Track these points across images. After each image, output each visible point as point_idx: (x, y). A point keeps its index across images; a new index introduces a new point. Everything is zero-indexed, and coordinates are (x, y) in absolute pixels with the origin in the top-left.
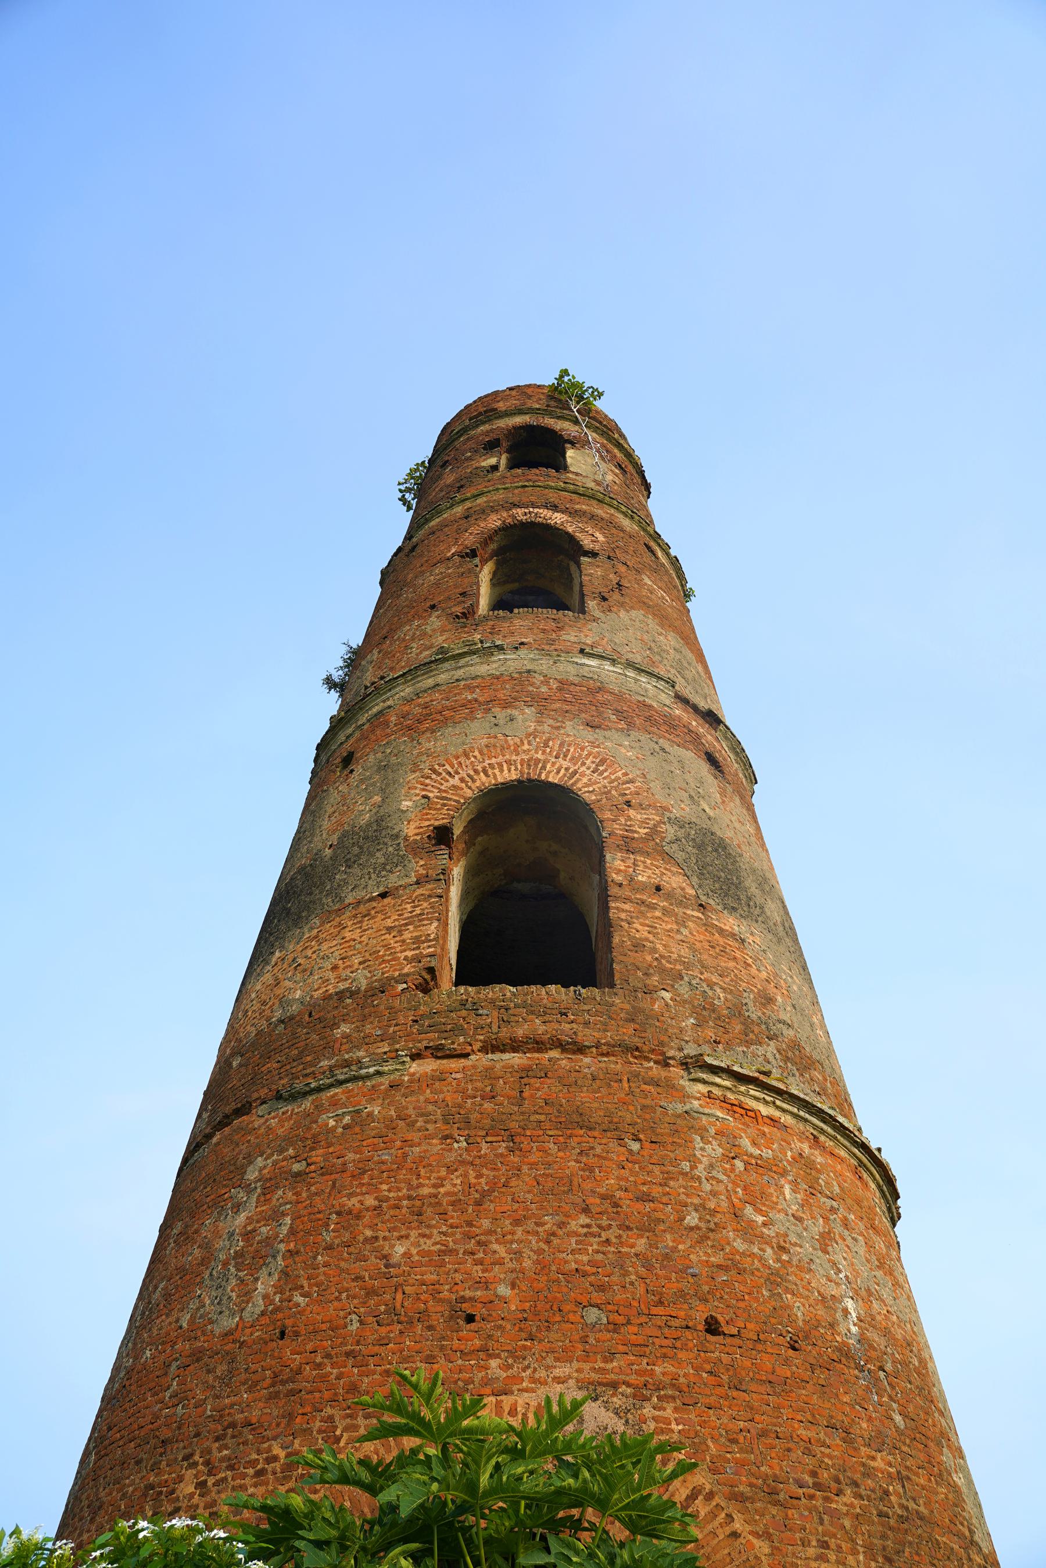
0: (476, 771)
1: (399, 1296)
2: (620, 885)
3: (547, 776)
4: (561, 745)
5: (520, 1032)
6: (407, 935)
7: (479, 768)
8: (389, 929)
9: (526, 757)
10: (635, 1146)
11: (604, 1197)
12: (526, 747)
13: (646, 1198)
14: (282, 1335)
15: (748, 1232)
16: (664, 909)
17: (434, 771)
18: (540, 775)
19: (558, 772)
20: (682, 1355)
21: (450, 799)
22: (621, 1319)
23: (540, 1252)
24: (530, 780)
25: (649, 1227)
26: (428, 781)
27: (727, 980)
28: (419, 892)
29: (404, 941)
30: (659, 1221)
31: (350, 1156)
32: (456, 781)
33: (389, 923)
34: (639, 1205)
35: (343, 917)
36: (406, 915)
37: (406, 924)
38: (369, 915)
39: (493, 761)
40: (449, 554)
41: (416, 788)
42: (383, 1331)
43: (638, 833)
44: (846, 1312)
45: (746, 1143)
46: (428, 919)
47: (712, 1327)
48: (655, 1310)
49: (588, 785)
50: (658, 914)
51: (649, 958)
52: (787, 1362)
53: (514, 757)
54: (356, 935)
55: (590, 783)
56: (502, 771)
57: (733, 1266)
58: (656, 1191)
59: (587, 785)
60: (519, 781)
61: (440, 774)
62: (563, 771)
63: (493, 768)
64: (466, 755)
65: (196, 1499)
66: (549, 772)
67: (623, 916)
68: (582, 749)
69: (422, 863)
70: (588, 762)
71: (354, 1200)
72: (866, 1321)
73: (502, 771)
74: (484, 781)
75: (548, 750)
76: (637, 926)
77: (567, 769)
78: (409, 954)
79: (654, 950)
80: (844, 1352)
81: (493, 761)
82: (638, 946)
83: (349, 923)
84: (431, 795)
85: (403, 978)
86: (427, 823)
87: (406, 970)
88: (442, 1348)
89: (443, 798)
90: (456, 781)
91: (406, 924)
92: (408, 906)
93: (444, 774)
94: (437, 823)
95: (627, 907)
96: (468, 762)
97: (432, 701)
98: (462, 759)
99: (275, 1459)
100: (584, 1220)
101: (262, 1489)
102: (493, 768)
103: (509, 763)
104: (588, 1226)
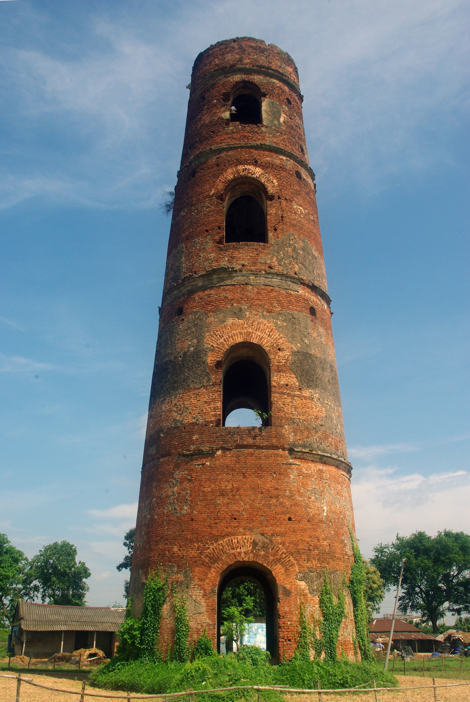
0: (229, 336)
1: (219, 514)
2: (275, 387)
3: (253, 341)
4: (258, 325)
5: (245, 443)
6: (211, 406)
7: (230, 335)
8: (206, 402)
9: (246, 331)
10: (275, 476)
11: (266, 490)
12: (246, 326)
13: (277, 489)
14: (192, 520)
15: (301, 495)
16: (288, 394)
17: (214, 333)
18: (250, 340)
19: (257, 338)
20: (282, 526)
21: (221, 349)
22: (269, 519)
23: (251, 504)
24: (247, 342)
25: (277, 497)
26: (213, 338)
27: (305, 417)
28: (214, 389)
29: (211, 408)
30: (279, 495)
31: (203, 477)
32: (222, 340)
33: (205, 399)
34: (275, 491)
35: (190, 393)
36: (211, 398)
37: (211, 402)
38: (198, 395)
39: (235, 332)
40: (211, 194)
41: (209, 341)
42: (216, 521)
43: (282, 362)
44: (324, 510)
45: (304, 470)
46: (218, 400)
47: (290, 519)
48: (277, 516)
49: (266, 344)
50: (286, 396)
51: (282, 414)
52: (306, 525)
53: (242, 331)
54: (195, 401)
55: (268, 341)
56: (238, 337)
57: (296, 505)
58: (279, 487)
59: (266, 343)
60: (243, 342)
61: (217, 336)
62: (258, 337)
63: (235, 336)
64: (225, 328)
65: (178, 552)
66: (254, 338)
67: (275, 399)
68: (265, 325)
69: (214, 377)
70: (267, 331)
71: (206, 489)
72: (330, 511)
73: (238, 337)
74: (231, 342)
75: (253, 327)
76: (280, 403)
77: (260, 336)
78: (213, 413)
79: (284, 411)
80: (321, 521)
81: (235, 332)
82: (279, 410)
83: (193, 396)
84: (214, 346)
85: (212, 422)
86: (214, 359)
87: (212, 419)
88: (230, 526)
89: (219, 348)
90: (222, 340)
91: (211, 402)
92: (211, 394)
93: (218, 336)
94: (218, 359)
95: (276, 395)
96: (226, 331)
97: (211, 294)
98: (224, 329)
99: (195, 546)
100: (261, 495)
101: (193, 552)
102: (235, 336)
103: (241, 333)
104: (263, 497)
